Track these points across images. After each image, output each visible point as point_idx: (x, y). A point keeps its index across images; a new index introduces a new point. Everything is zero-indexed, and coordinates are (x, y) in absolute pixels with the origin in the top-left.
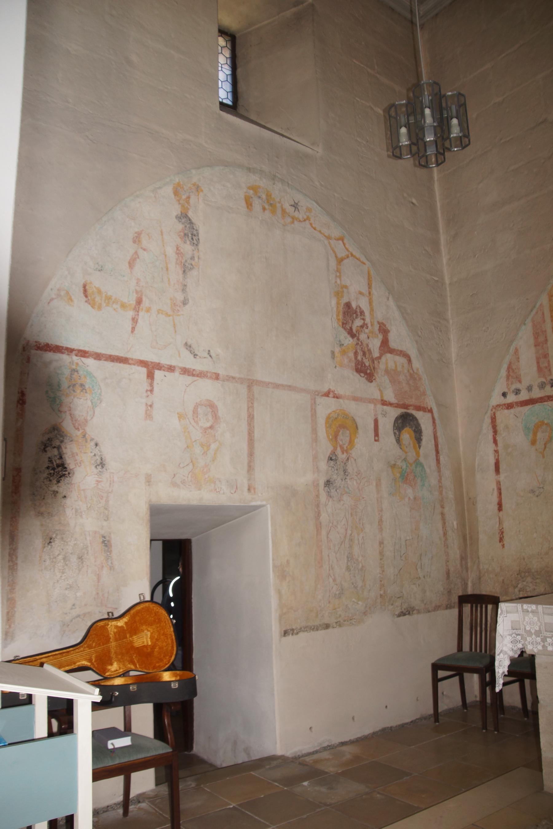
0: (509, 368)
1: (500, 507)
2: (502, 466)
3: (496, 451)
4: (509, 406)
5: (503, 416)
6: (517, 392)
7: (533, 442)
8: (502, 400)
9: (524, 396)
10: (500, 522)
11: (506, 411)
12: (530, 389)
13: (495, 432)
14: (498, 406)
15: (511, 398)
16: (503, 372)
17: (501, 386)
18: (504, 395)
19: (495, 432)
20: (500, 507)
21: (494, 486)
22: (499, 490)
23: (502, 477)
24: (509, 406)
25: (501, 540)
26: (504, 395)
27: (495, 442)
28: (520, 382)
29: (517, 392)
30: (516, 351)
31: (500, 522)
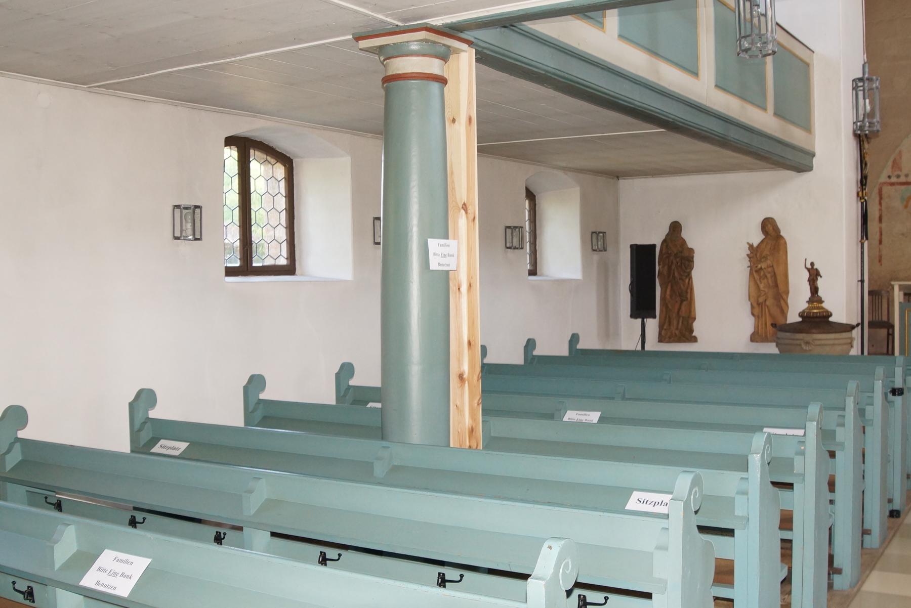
0: (894, 162)
1: (880, 242)
2: (884, 219)
3: (880, 210)
4: (892, 184)
5: (886, 190)
6: (898, 176)
7: (906, 207)
8: (888, 180)
9: (902, 179)
10: (880, 251)
11: (889, 187)
12: (907, 176)
13: (881, 198)
14: (885, 183)
15: (894, 180)
16: (890, 163)
17: (887, 171)
18: (889, 177)
19: (881, 198)
20: (880, 242)
21: (878, 229)
22: (881, 234)
23: (883, 225)
24: (892, 184)
25: (880, 261)
26: (889, 177)
27: (880, 204)
28: (901, 171)
29: (898, 176)
30: (900, 152)
31: (880, 251)
